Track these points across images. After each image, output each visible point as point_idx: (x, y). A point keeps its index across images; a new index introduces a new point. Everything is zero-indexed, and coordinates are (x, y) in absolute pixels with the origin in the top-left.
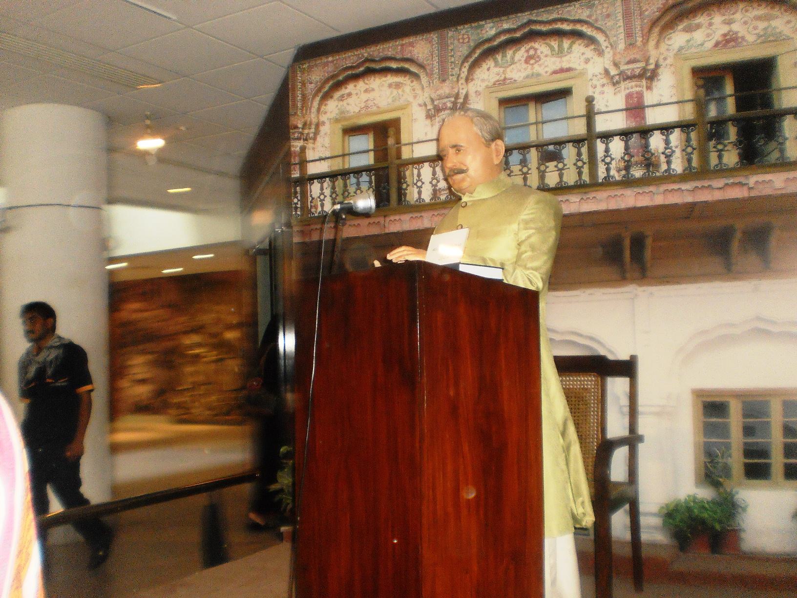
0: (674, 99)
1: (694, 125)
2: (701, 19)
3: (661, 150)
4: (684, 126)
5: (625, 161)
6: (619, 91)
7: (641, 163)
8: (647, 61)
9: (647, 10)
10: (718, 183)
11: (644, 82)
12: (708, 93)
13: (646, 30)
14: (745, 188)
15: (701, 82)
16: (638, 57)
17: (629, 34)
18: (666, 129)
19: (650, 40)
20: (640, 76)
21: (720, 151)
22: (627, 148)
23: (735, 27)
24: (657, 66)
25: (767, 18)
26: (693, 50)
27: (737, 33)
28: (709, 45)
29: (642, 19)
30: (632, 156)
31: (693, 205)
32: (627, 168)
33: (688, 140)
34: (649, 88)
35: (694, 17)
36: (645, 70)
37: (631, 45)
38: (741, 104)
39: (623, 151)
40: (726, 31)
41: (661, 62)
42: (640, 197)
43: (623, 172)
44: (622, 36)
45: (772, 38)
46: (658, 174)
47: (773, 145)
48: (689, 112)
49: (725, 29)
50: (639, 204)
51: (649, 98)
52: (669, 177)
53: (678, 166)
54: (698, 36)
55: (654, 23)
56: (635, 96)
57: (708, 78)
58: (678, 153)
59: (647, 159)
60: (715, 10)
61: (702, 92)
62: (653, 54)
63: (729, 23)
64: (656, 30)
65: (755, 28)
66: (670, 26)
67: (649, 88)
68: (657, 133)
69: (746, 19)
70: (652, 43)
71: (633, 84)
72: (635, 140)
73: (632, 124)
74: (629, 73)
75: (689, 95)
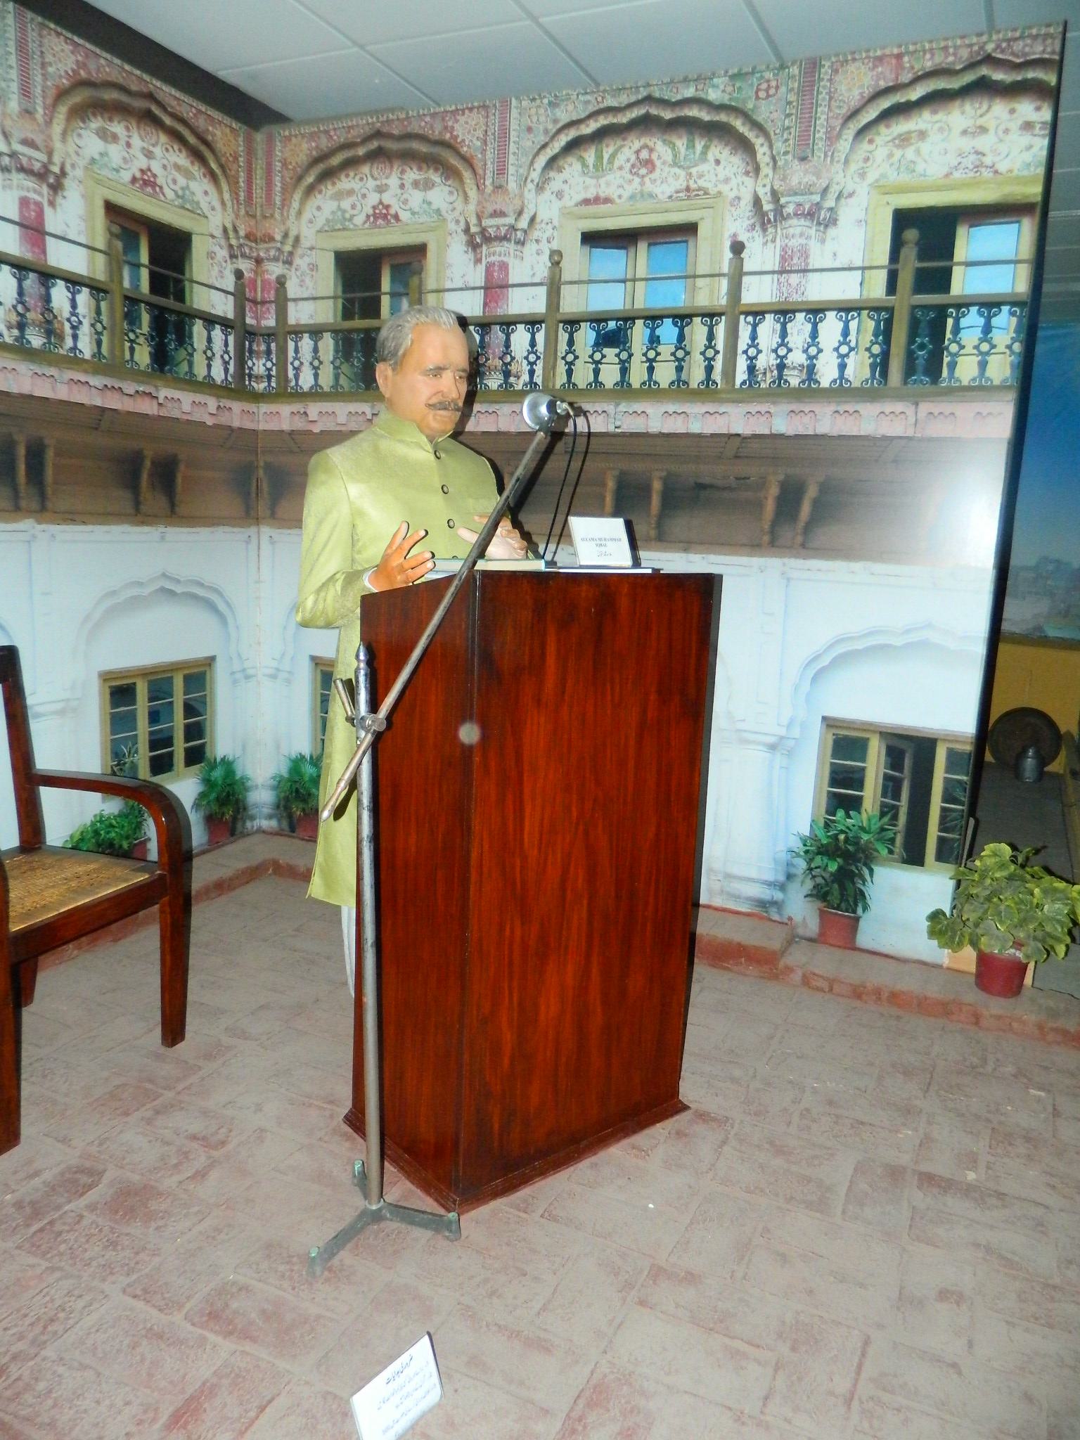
0: (83, 240)
1: (105, 292)
2: (118, 128)
3: (66, 314)
4: (97, 290)
5: (19, 314)
6: (10, 187)
7: (40, 326)
8: (50, 154)
9: (50, 64)
10: (130, 387)
11: (45, 189)
12: (125, 252)
13: (49, 101)
14: (155, 402)
15: (116, 229)
16: (39, 139)
17: (26, 92)
18: (74, 282)
19: (55, 121)
20: (41, 176)
21: (132, 341)
22: (21, 292)
23: (156, 167)
24: (63, 173)
25: (188, 175)
26: (105, 172)
27: (155, 176)
28: (126, 176)
29: (45, 76)
30: (28, 310)
31: (103, 410)
32: (21, 326)
33: (98, 312)
34: (52, 204)
35: (111, 120)
36: (45, 166)
37: (28, 113)
38: (158, 284)
39: (16, 296)
40: (144, 167)
41: (68, 168)
42: (39, 381)
43: (16, 332)
44: (14, 87)
45: (188, 206)
46: (61, 352)
47: (182, 354)
48: (97, 268)
49: (142, 162)
50: (38, 393)
51: (52, 222)
52: (73, 360)
53: (86, 347)
54: (115, 152)
55: (62, 94)
56: (32, 207)
57: (125, 223)
58: (85, 329)
59: (48, 322)
60: (134, 125)
61: (119, 245)
62: (58, 145)
63: (149, 155)
64: (63, 110)
65: (175, 181)
66: (80, 113)
67: (52, 204)
68: (61, 283)
69: (165, 162)
70: (57, 128)
71: (31, 184)
72: (31, 281)
73: (28, 256)
74: (24, 161)
75: (100, 243)
